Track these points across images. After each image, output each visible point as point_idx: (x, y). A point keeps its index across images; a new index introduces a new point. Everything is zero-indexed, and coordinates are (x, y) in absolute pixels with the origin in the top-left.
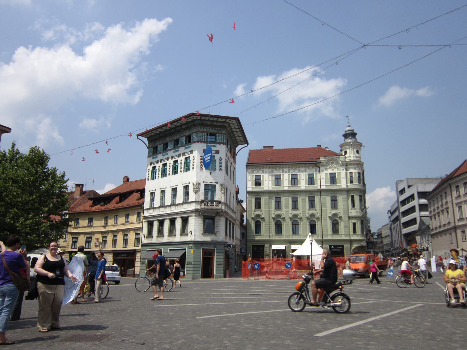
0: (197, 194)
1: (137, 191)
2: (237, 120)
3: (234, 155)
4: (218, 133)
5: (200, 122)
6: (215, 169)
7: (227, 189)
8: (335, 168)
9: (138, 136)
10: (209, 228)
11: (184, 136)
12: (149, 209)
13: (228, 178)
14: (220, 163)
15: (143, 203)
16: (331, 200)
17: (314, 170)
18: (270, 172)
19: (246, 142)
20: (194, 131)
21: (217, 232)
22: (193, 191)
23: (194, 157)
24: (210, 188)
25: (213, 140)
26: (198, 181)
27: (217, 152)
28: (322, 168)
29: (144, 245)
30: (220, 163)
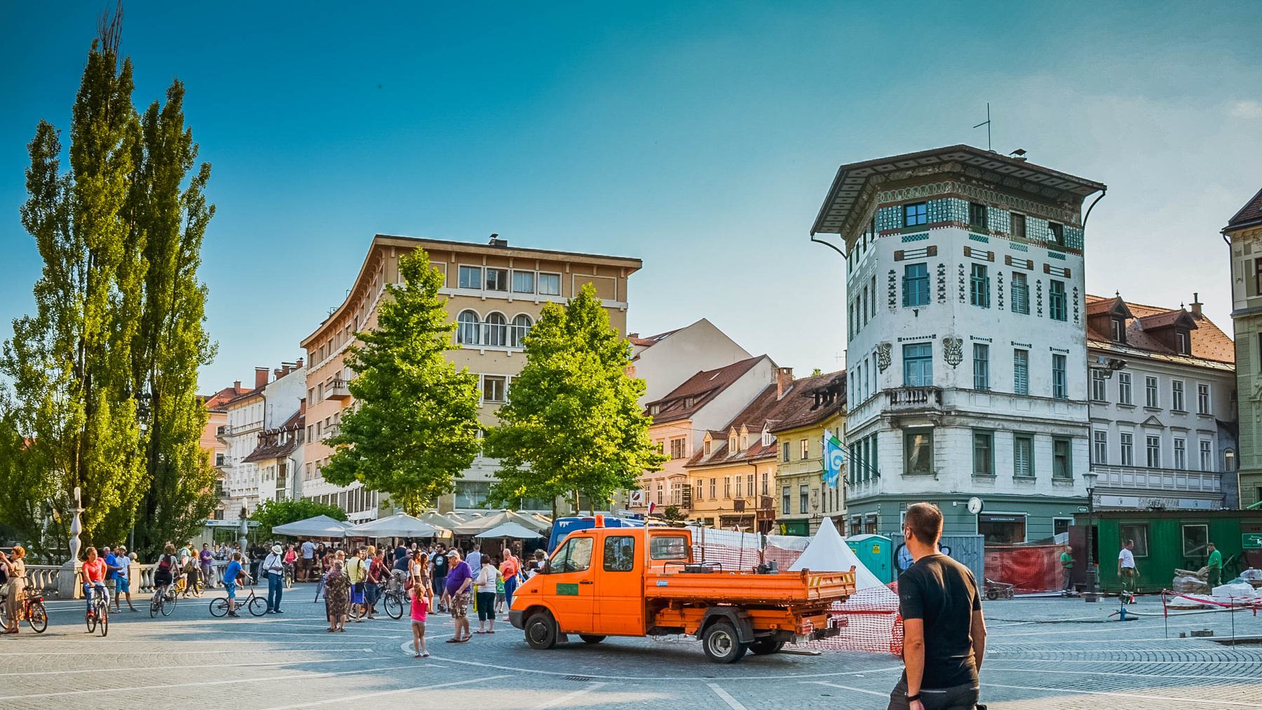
5: (880, 179)
10: (920, 461)
12: (850, 415)
14: (942, 281)
21: (939, 468)
24: (916, 353)
26: (886, 340)
27: (932, 251)
29: (850, 504)
30: (942, 281)
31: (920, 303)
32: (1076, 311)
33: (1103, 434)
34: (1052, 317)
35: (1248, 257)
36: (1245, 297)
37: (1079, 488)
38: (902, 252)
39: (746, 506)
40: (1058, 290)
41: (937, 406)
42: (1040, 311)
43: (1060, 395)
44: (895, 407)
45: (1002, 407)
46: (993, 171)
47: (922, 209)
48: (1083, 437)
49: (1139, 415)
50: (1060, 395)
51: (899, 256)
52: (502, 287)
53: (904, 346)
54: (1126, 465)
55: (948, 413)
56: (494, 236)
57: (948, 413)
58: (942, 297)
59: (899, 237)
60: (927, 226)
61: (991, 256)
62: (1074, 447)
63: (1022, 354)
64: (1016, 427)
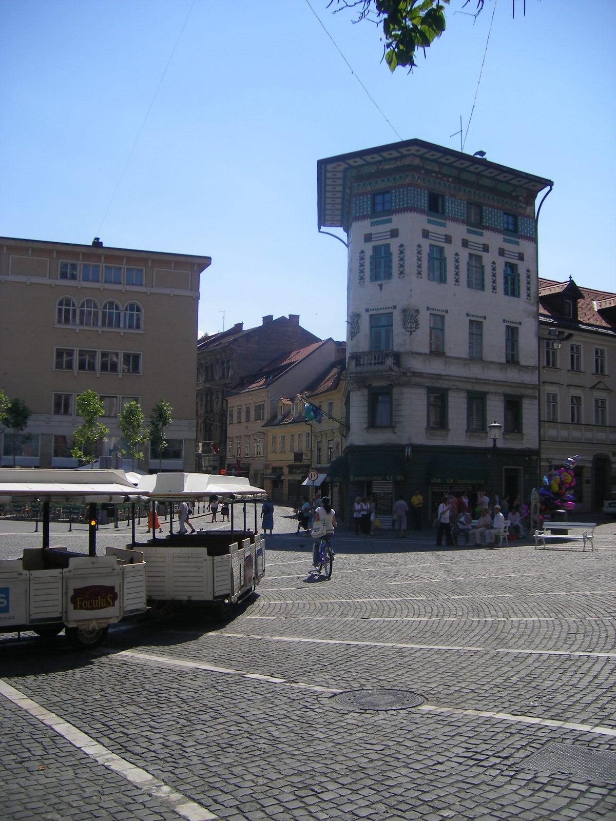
6: (389, 276)
30: (402, 259)
31: (384, 279)
32: (528, 289)
33: (555, 396)
34: (506, 293)
37: (529, 439)
39: (304, 457)
40: (513, 271)
41: (395, 368)
42: (494, 288)
43: (512, 360)
44: (359, 369)
45: (456, 370)
46: (450, 165)
47: (387, 196)
48: (533, 397)
49: (589, 379)
50: (512, 360)
52: (73, 277)
53: (371, 316)
54: (575, 421)
55: (404, 374)
56: (97, 239)
57: (404, 374)
59: (367, 222)
61: (448, 239)
62: (450, 399)
63: (476, 326)
64: (470, 387)
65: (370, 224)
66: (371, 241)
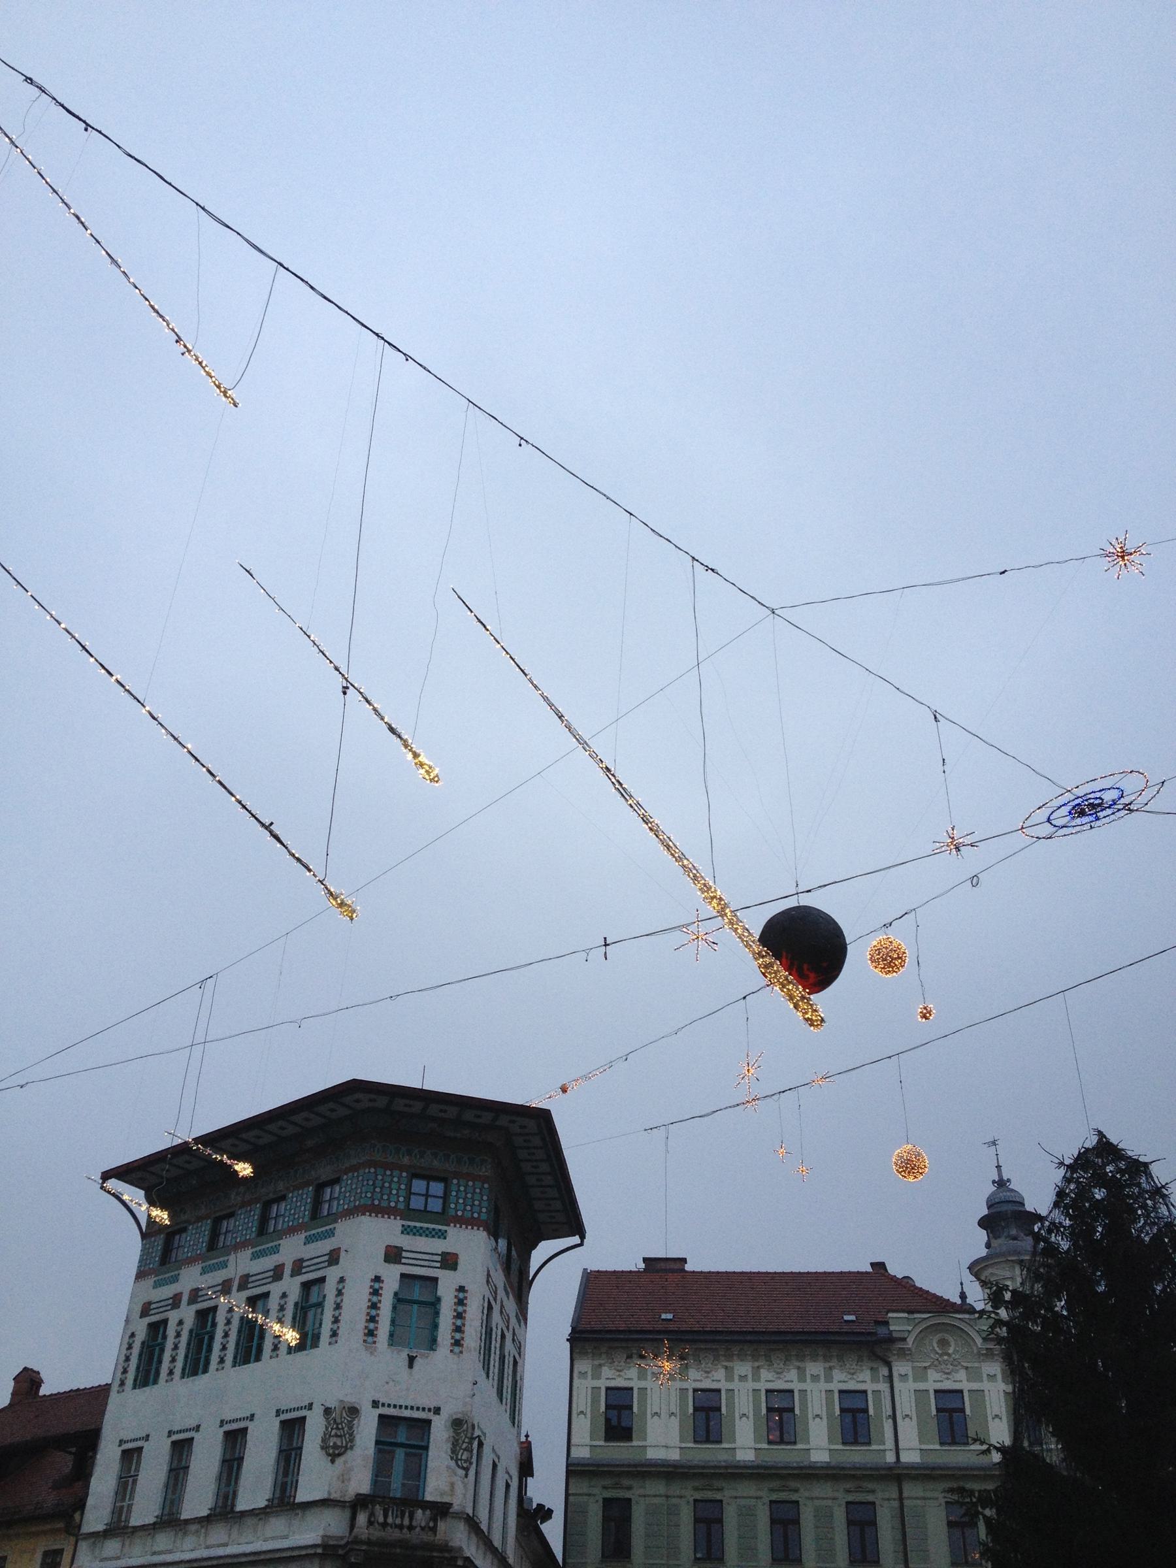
0: (340, 1461)
1: (60, 1442)
2: (543, 1117)
3: (520, 1283)
4: (457, 1175)
6: (432, 1343)
7: (481, 1445)
8: (955, 1364)
9: (106, 1176)
11: (307, 1184)
13: (488, 1388)
15: (81, 1505)
16: (950, 1524)
17: (866, 1375)
18: (672, 1378)
19: (573, 1225)
20: (354, 1162)
22: (324, 1447)
23: (342, 1280)
24: (403, 1434)
25: (435, 1205)
26: (351, 1399)
27: (449, 1261)
28: (901, 1367)
30: (459, 1316)
35: (596, 1383)
36: (587, 1441)
38: (400, 1250)
47: (437, 1188)
51: (393, 1255)
53: (381, 1416)
58: (457, 1343)
59: (397, 1224)
60: (445, 1217)
65: (400, 1228)
66: (400, 1263)
